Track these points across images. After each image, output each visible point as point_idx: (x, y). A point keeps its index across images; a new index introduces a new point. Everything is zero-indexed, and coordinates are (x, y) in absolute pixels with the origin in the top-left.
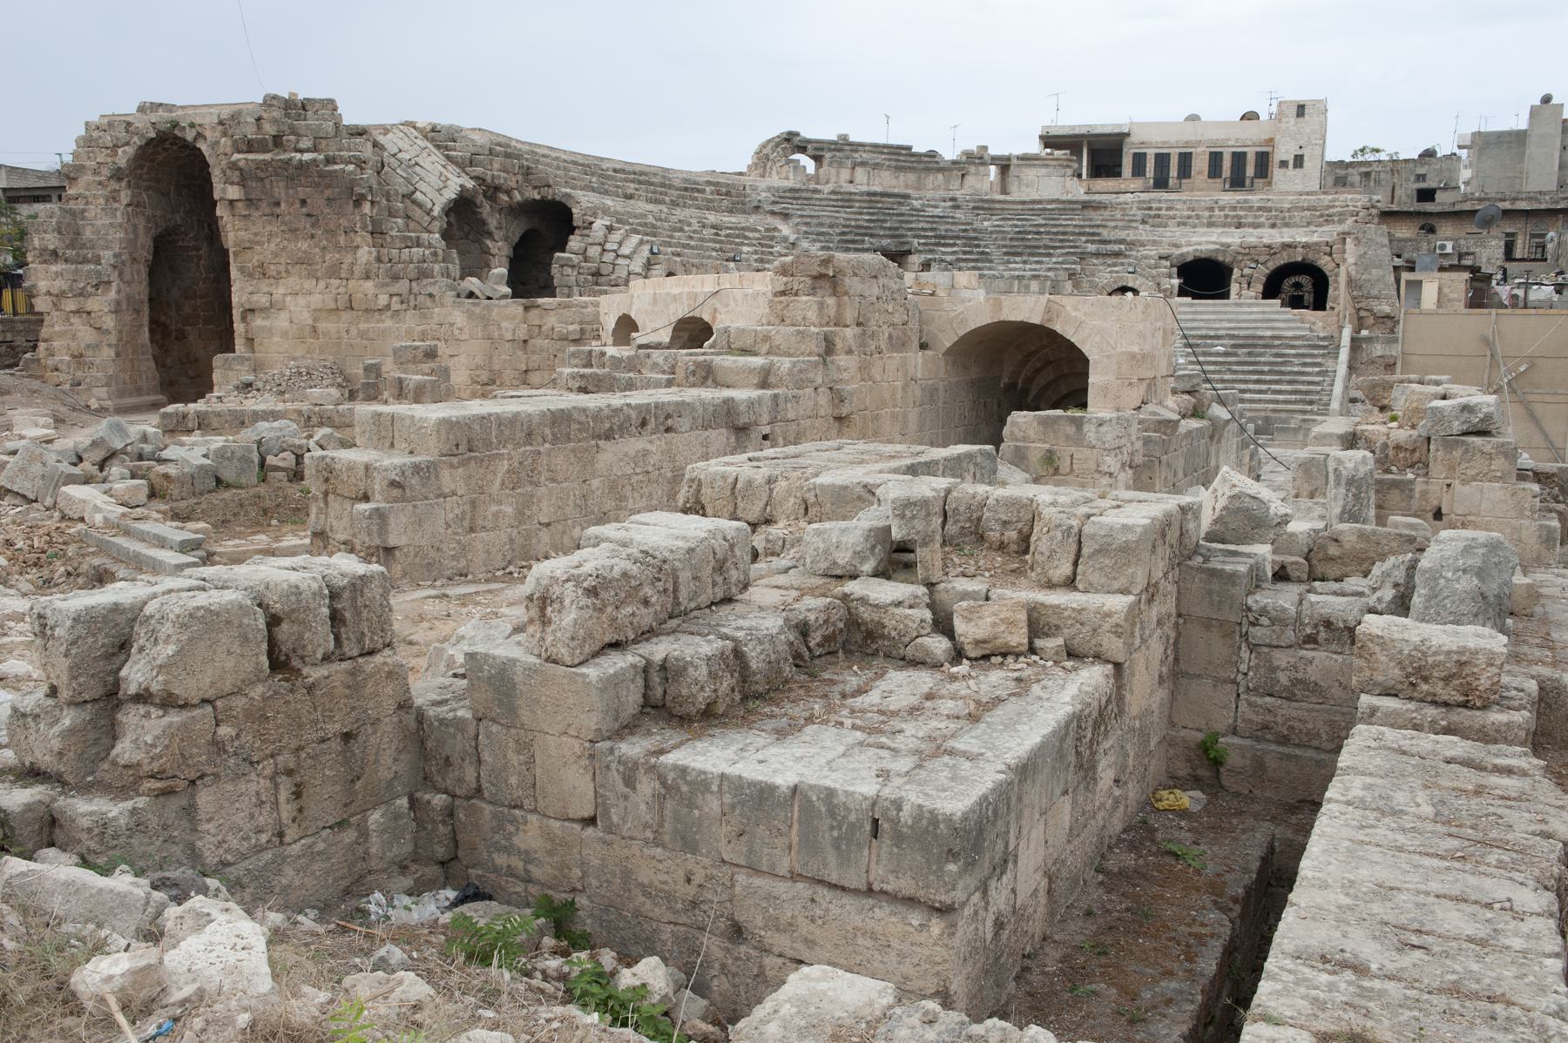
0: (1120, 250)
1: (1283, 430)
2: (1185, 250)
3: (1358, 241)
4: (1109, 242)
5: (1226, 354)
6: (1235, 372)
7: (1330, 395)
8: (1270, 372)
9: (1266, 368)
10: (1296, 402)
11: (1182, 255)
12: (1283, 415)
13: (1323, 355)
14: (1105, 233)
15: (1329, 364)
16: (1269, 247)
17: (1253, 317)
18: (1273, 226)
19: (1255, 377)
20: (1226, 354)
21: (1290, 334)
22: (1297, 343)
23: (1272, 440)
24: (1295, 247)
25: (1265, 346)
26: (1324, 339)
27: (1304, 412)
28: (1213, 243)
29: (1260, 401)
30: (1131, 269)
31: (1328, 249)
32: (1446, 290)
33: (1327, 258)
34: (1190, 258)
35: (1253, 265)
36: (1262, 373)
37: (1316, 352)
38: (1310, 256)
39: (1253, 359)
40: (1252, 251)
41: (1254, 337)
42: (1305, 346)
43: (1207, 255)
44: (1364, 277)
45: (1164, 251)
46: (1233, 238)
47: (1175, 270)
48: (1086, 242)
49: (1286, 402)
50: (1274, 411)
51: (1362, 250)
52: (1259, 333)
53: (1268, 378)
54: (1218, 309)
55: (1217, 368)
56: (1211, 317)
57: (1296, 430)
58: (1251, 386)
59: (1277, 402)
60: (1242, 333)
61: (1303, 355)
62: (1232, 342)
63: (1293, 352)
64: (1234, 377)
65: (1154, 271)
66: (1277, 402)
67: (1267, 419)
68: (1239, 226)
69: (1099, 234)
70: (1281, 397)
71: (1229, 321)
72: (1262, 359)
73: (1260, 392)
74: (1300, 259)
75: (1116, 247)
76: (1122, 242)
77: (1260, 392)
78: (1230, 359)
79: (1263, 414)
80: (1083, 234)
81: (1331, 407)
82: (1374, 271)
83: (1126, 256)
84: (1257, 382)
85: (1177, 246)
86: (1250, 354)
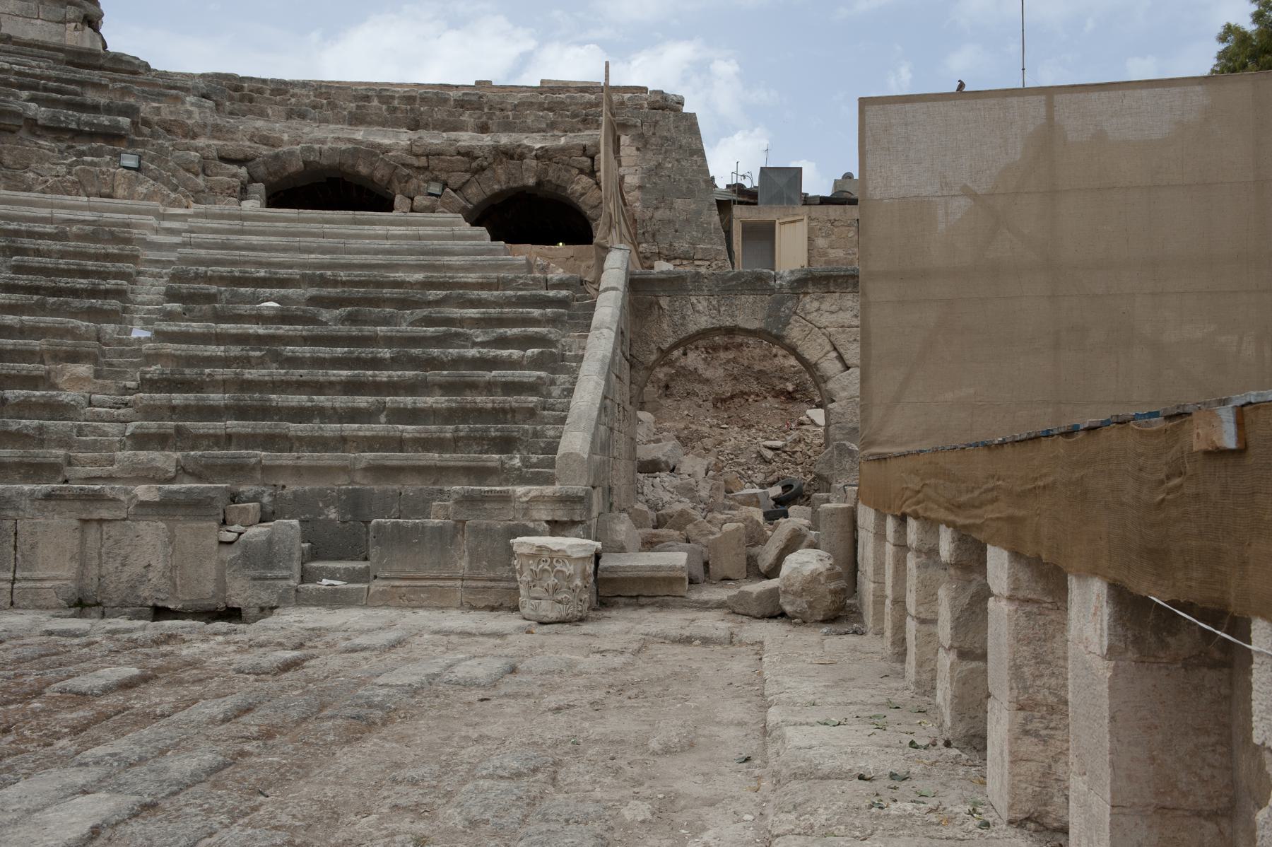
0: (117, 126)
1: (400, 538)
2: (285, 148)
3: (643, 143)
4: (95, 108)
5: (283, 318)
6: (294, 362)
7: (563, 420)
8: (395, 363)
9: (386, 353)
10: (455, 444)
11: (277, 157)
12: (411, 486)
13: (553, 321)
14: (91, 96)
15: (566, 339)
16: (468, 154)
17: (387, 244)
18: (483, 129)
19: (345, 373)
20: (283, 318)
21: (472, 277)
22: (485, 294)
23: (363, 576)
24: (522, 157)
25: (403, 304)
26: (561, 285)
27: (480, 473)
28: (350, 140)
29: (342, 442)
30: (130, 161)
31: (586, 162)
32: (821, 242)
33: (586, 180)
34: (296, 166)
35: (435, 188)
36: (376, 363)
37: (536, 312)
38: (552, 175)
39: (354, 330)
40: (434, 162)
41: (380, 284)
42: (509, 303)
43: (325, 162)
44: (659, 214)
45: (230, 147)
46: (397, 139)
47: (260, 187)
48: (32, 100)
49: (425, 444)
50: (378, 471)
51: (652, 159)
52: (399, 275)
53: (383, 376)
54: (301, 227)
55: (235, 350)
56: (274, 240)
57: (445, 537)
58: (322, 400)
59: (400, 444)
60: (343, 275)
61: (501, 322)
62: (313, 291)
63: (472, 312)
64: (278, 373)
65: (200, 181)
66: (400, 444)
67: (356, 504)
68: (415, 126)
69: (76, 94)
70: (409, 430)
71: (323, 251)
72: (381, 330)
73: (354, 415)
74: (531, 181)
75: (105, 120)
76: (130, 111)
77: (354, 415)
78: (285, 329)
79: (342, 483)
80: (22, 87)
81: (562, 450)
82: (679, 203)
83: (132, 144)
84: (352, 387)
85: (266, 141)
86: (352, 319)
